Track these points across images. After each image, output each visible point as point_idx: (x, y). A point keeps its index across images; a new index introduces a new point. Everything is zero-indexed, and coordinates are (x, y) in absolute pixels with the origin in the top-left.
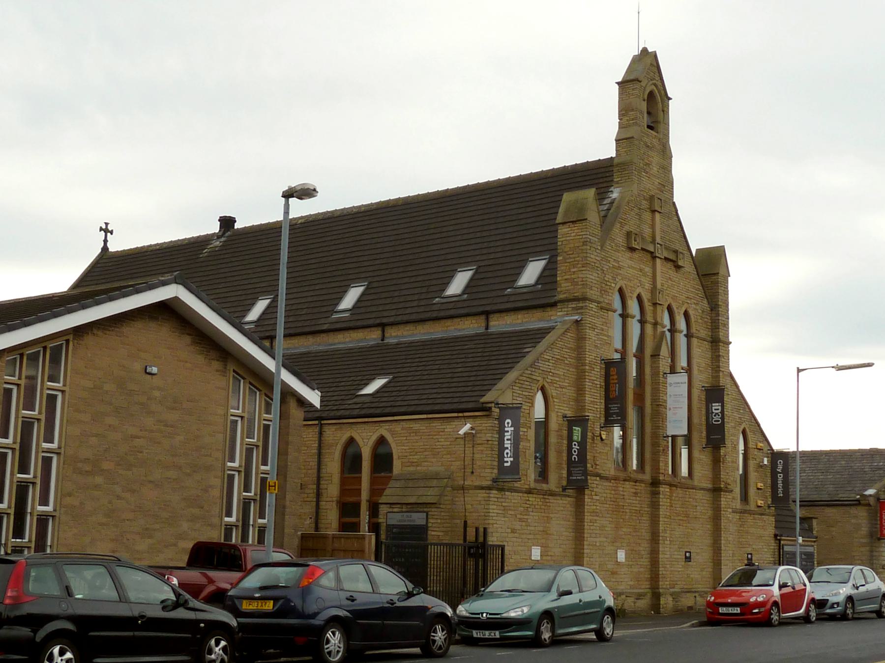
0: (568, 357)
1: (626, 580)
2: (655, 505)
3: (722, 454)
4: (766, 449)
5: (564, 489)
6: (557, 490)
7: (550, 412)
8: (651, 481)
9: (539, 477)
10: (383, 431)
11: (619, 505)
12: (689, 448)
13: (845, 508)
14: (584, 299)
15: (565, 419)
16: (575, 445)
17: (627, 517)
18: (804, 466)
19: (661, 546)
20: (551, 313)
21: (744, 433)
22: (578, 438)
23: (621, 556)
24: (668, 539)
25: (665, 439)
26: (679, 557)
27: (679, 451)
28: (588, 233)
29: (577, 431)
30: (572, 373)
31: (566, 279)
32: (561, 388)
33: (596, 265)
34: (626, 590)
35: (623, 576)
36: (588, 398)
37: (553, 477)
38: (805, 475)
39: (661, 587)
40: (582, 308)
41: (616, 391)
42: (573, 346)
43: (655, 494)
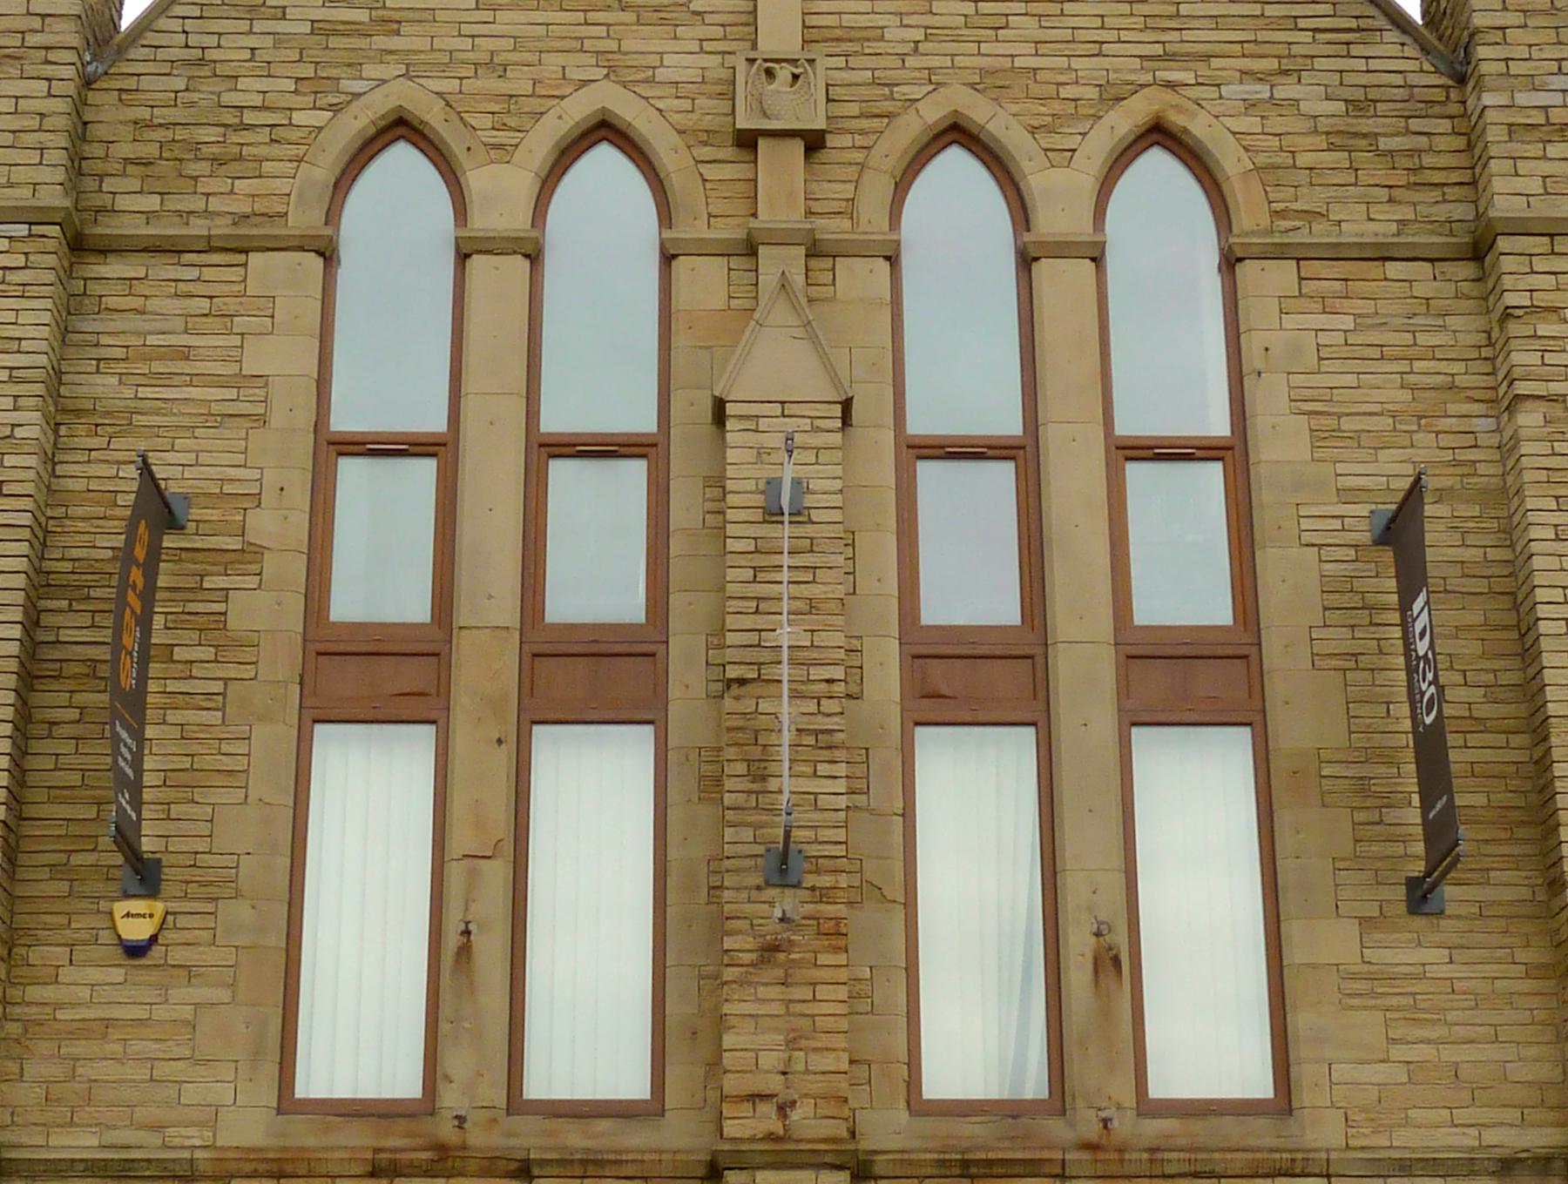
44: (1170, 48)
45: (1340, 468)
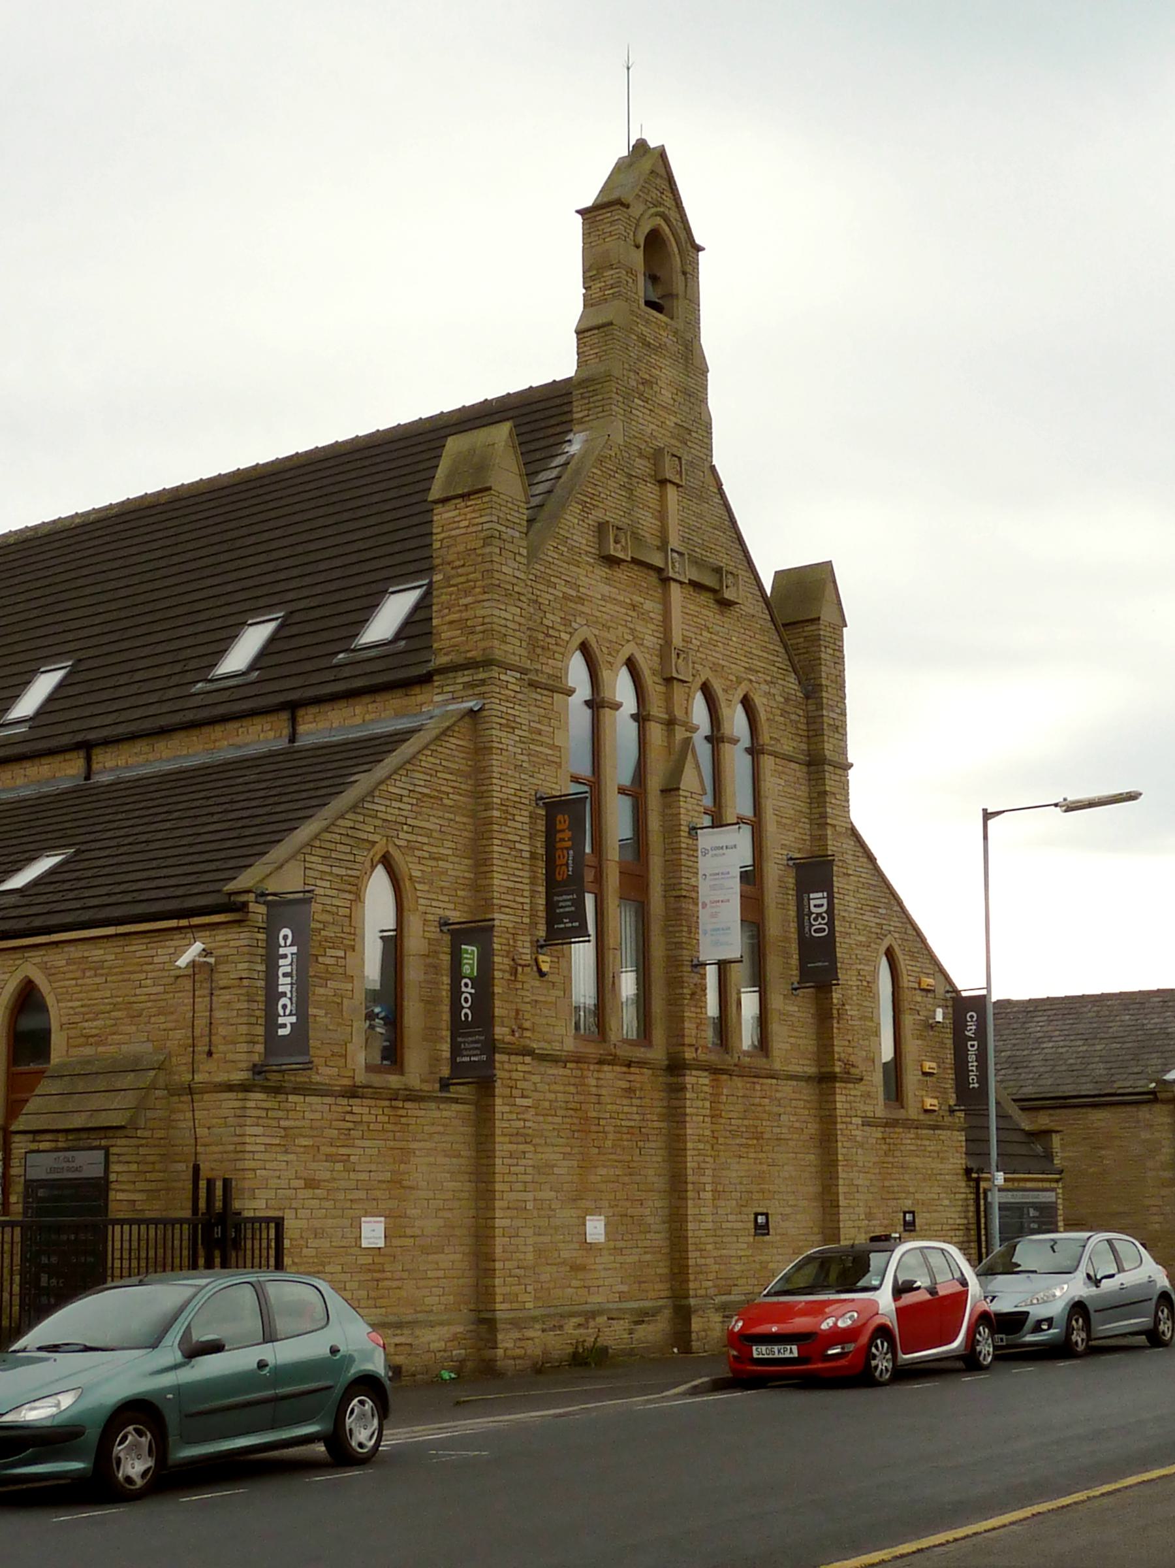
0: (451, 790)
2: (675, 1116)
3: (835, 1001)
4: (941, 990)
5: (445, 1085)
6: (426, 1087)
7: (405, 913)
8: (666, 1063)
9: (383, 1058)
10: (30, 968)
11: (587, 1119)
12: (759, 991)
13: (1129, 1109)
14: (487, 663)
15: (445, 929)
16: (466, 985)
17: (609, 1143)
18: (1050, 1028)
19: (690, 1203)
20: (420, 698)
21: (890, 954)
22: (472, 969)
23: (596, 1229)
24: (708, 1187)
25: (695, 970)
26: (739, 1225)
27: (734, 996)
28: (495, 519)
29: (470, 953)
30: (462, 827)
31: (451, 622)
32: (434, 859)
33: (516, 588)
34: (611, 1306)
35: (603, 1274)
36: (499, 881)
37: (416, 1060)
38: (1051, 1045)
39: (691, 1293)
40: (483, 682)
41: (567, 865)
42: (462, 767)
43: (676, 1090)
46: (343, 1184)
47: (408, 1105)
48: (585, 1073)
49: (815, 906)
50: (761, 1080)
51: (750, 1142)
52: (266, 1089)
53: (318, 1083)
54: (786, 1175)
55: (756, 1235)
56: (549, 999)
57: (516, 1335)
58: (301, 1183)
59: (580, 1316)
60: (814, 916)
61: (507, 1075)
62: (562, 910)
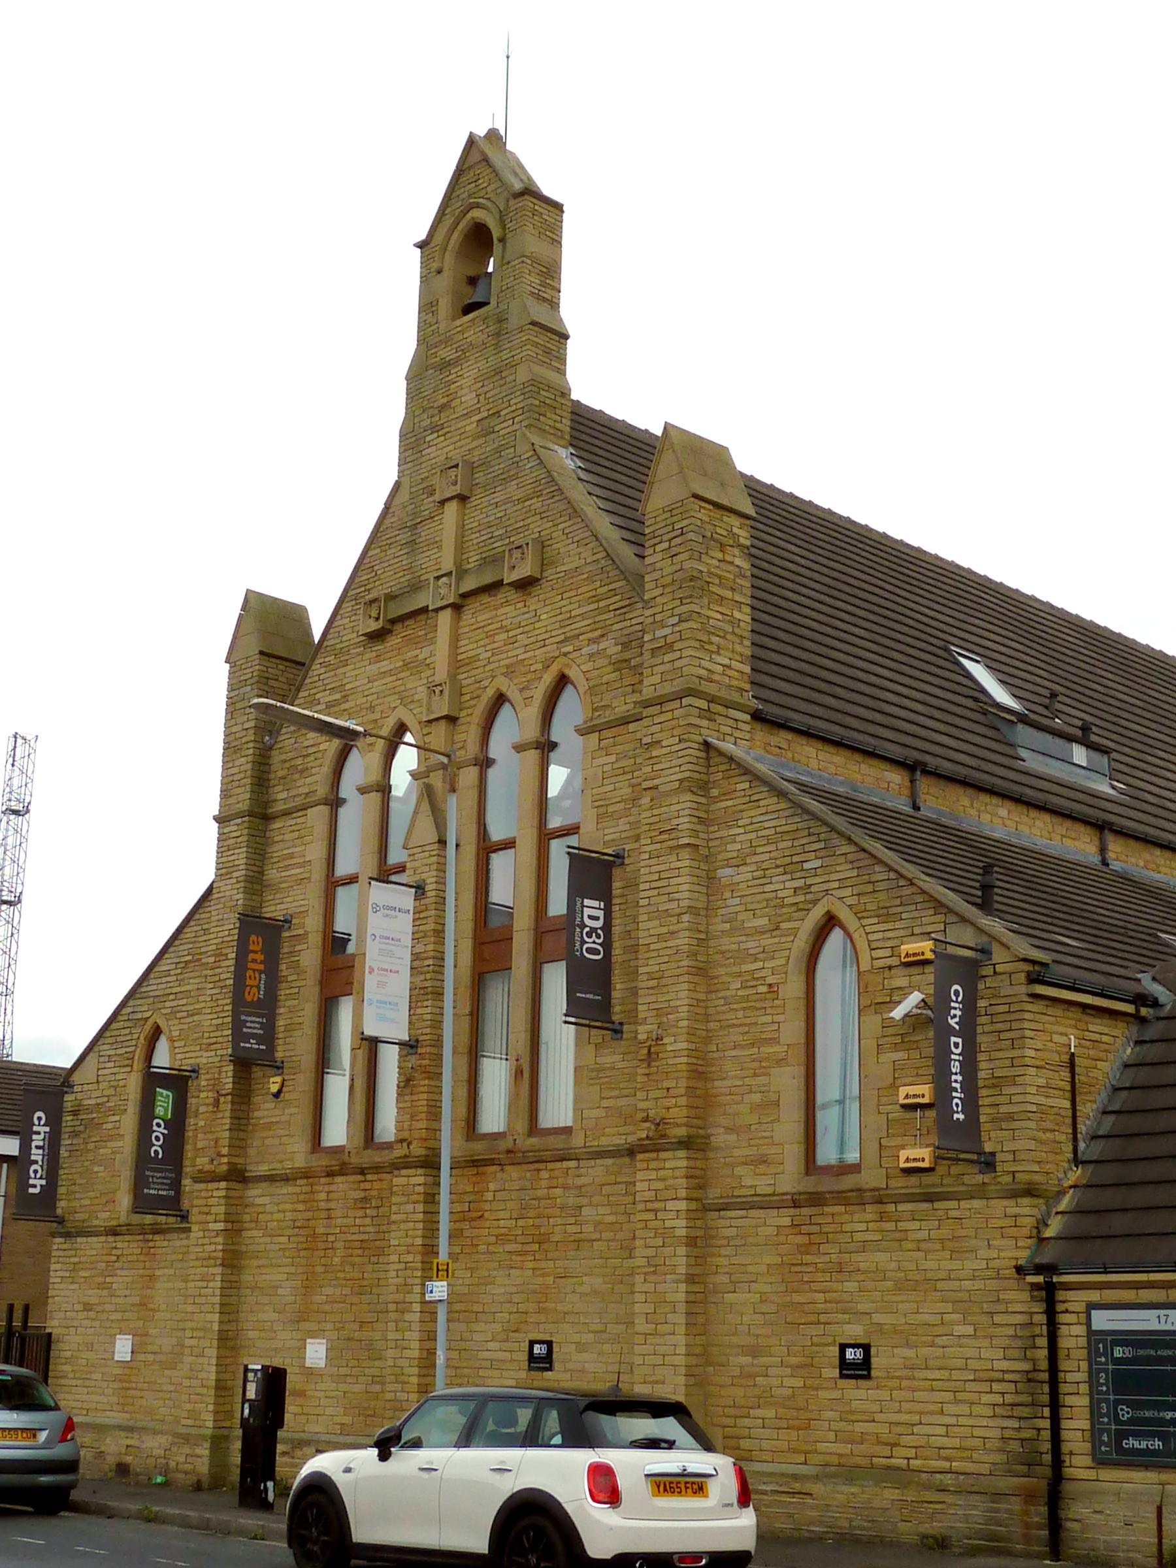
1: (329, 1411)
17: (336, 1260)
44: (568, 635)
45: (606, 832)
46: (107, 1307)
47: (157, 1237)
48: (315, 1187)
49: (590, 917)
50: (550, 1166)
51: (527, 1248)
52: (62, 1235)
53: (95, 1226)
54: (586, 1289)
55: (530, 1369)
56: (283, 1118)
57: (186, 1450)
58: (78, 1307)
59: (285, 1443)
60: (587, 929)
61: (203, 1202)
62: (249, 1030)
